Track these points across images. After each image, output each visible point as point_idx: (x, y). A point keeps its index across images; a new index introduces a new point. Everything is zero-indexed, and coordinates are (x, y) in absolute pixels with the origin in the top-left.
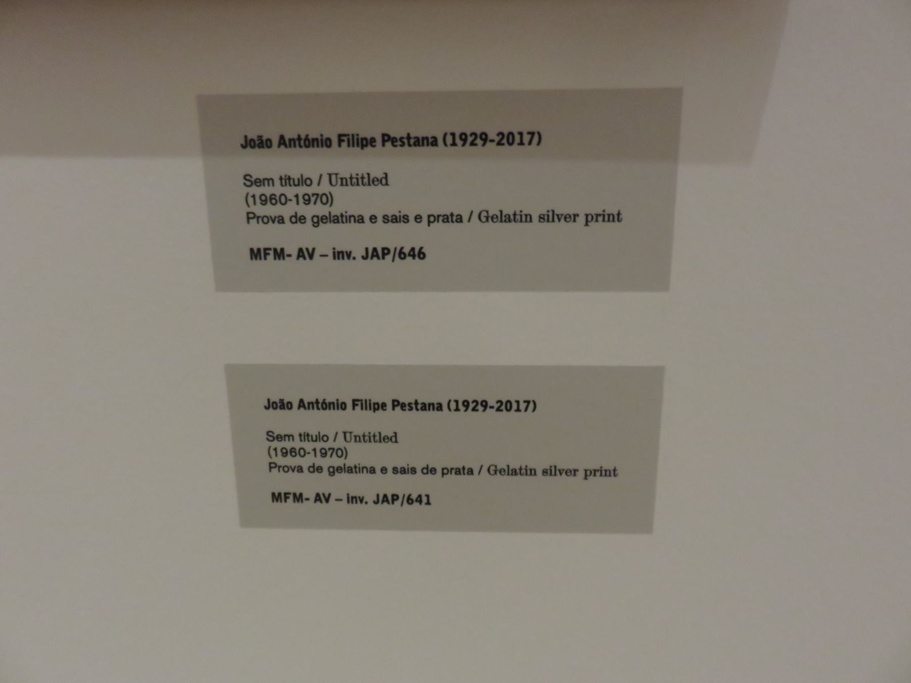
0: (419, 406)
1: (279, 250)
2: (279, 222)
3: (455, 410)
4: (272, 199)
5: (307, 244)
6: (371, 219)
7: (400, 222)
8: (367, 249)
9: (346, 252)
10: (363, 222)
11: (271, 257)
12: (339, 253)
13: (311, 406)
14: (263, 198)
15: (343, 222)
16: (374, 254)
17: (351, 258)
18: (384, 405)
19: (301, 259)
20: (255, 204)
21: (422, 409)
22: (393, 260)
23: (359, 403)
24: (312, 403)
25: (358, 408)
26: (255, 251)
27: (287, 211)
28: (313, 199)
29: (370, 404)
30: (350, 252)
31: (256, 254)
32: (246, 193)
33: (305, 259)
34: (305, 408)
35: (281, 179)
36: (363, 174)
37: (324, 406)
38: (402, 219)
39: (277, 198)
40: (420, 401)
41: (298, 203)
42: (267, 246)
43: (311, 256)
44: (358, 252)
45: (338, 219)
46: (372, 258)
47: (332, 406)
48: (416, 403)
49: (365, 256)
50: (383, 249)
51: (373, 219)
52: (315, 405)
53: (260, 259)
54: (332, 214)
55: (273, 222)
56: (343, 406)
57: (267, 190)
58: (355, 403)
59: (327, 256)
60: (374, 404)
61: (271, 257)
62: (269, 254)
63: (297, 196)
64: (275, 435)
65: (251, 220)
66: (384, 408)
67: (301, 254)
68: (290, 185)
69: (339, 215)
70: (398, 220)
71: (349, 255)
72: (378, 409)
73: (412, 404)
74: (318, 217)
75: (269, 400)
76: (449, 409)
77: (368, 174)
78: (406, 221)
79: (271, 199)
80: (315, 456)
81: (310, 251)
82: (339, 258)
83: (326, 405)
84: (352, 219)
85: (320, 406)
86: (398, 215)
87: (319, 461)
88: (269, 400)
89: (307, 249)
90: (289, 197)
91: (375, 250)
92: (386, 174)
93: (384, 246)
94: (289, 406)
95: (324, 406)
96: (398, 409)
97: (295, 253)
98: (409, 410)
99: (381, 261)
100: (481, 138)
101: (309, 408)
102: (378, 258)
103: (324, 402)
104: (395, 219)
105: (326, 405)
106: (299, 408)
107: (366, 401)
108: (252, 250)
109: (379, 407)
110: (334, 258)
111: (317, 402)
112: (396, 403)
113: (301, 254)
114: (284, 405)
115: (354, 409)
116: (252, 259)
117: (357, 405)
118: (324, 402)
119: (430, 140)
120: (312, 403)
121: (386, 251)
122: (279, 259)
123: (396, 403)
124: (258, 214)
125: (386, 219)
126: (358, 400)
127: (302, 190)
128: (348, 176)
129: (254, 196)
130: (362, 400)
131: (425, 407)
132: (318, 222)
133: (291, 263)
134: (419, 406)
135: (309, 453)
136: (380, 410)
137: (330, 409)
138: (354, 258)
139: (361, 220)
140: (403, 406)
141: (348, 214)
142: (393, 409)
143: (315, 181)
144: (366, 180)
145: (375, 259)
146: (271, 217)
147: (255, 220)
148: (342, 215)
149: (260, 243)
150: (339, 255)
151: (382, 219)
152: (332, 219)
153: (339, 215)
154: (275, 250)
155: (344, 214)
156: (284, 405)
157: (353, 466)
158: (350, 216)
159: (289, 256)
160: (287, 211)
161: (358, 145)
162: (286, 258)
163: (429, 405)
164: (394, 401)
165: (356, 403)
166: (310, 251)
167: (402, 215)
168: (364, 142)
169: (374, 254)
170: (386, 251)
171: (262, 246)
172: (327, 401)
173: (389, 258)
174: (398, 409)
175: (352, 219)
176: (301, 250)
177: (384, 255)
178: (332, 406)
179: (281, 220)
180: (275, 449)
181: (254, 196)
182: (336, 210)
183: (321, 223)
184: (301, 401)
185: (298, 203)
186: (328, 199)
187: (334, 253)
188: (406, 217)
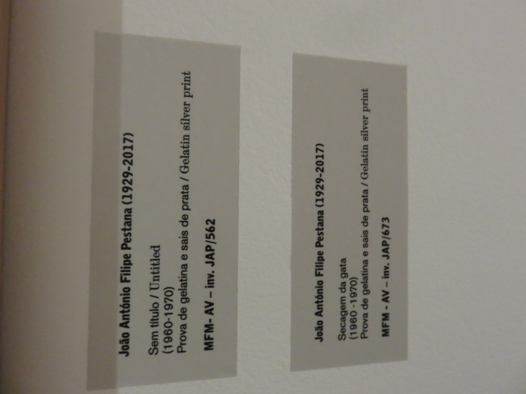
1: (206, 329)
2: (185, 328)
3: (323, 202)
4: (168, 333)
6: (184, 259)
7: (187, 237)
8: (207, 262)
9: (209, 278)
10: (186, 265)
11: (211, 335)
12: (209, 283)
13: (320, 307)
14: (167, 340)
15: (186, 280)
16: (210, 257)
18: (320, 254)
19: (213, 312)
20: (171, 346)
21: (322, 225)
22: (215, 243)
23: (318, 271)
25: (322, 272)
26: (206, 346)
27: (177, 322)
28: (169, 302)
29: (319, 263)
30: (209, 275)
31: (209, 346)
33: (212, 309)
34: (322, 311)
35: (152, 326)
36: (151, 264)
37: (320, 297)
38: (185, 236)
39: (167, 329)
41: (171, 314)
43: (211, 304)
44: (209, 269)
46: (213, 259)
47: (320, 291)
48: (318, 229)
49: (212, 264)
50: (207, 250)
53: (212, 343)
54: (181, 288)
55: (185, 332)
56: (320, 283)
57: (161, 337)
58: (318, 275)
59: (211, 293)
60: (319, 260)
61: (211, 335)
62: (209, 336)
63: (166, 314)
64: (341, 334)
65: (184, 350)
66: (321, 253)
67: (209, 312)
68: (158, 319)
69: (180, 283)
70: (185, 239)
71: (211, 276)
72: (322, 257)
73: (318, 233)
74: (182, 299)
75: (316, 338)
76: (322, 206)
77: (151, 260)
79: (168, 334)
81: (207, 305)
82: (213, 283)
83: (320, 296)
84: (184, 273)
85: (320, 300)
86: (181, 239)
88: (316, 338)
89: (206, 307)
90: (167, 321)
91: (207, 256)
92: (152, 247)
94: (320, 323)
95: (320, 297)
96: (322, 243)
97: (209, 316)
98: (323, 235)
100: (127, 176)
102: (213, 254)
103: (317, 297)
104: (185, 241)
105: (320, 296)
106: (322, 316)
107: (316, 266)
108: (206, 349)
109: (321, 257)
110: (213, 287)
112: (318, 244)
113: (209, 312)
114: (320, 327)
116: (212, 349)
117: (319, 273)
118: (317, 297)
119: (127, 214)
120: (318, 306)
121: (208, 248)
124: (179, 345)
125: (185, 248)
126: (316, 272)
127: (162, 310)
128: (152, 276)
129: (166, 347)
130: (316, 269)
131: (321, 223)
132: (186, 298)
133: (216, 319)
134: (320, 227)
136: (323, 256)
137: (322, 293)
138: (213, 272)
140: (320, 239)
141: (180, 276)
142: (322, 246)
143: (155, 300)
144: (156, 262)
145: (214, 256)
146: (181, 334)
147: (183, 346)
148: (181, 280)
150: (210, 283)
152: (184, 288)
153: (180, 283)
154: (206, 331)
155: (180, 279)
156: (320, 327)
158: (182, 274)
159: (210, 321)
160: (177, 322)
161: (129, 268)
163: (319, 220)
164: (317, 246)
165: (318, 273)
166: (207, 305)
167: (181, 236)
168: (127, 263)
169: (210, 257)
170: (208, 248)
171: (203, 341)
172: (317, 295)
173: (213, 246)
174: (322, 243)
175: (184, 273)
176: (206, 312)
177: (211, 250)
178: (320, 291)
179: (184, 326)
180: (351, 334)
182: (177, 285)
183: (187, 297)
184: (317, 314)
185: (171, 314)
186: (169, 290)
187: (209, 287)
188: (183, 233)
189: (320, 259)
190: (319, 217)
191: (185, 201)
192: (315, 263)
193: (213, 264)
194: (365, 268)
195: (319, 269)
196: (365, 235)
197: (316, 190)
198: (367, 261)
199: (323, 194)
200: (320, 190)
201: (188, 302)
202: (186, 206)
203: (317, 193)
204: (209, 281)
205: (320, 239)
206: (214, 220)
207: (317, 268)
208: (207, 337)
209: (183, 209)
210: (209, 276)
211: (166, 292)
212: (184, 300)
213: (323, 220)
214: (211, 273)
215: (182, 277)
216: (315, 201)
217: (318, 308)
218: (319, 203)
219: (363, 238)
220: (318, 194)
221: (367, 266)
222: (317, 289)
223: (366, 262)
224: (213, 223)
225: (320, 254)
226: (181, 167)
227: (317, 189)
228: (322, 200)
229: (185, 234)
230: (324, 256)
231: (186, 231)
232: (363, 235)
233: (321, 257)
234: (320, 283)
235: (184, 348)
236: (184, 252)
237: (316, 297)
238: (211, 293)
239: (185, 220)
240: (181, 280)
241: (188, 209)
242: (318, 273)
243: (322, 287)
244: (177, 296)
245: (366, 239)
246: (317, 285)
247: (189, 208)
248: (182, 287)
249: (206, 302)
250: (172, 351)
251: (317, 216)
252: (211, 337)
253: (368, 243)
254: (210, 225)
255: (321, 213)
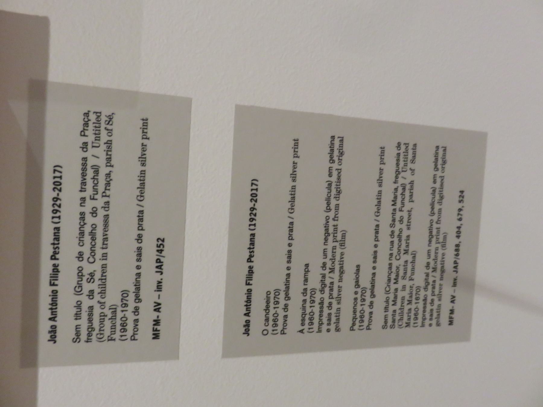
0: (252, 247)
1: (154, 323)
2: (138, 322)
5: (152, 307)
6: (138, 269)
9: (158, 284)
12: (158, 288)
16: (160, 268)
17: (161, 281)
18: (251, 268)
19: (160, 310)
23: (248, 281)
24: (247, 308)
25: (251, 282)
26: (154, 336)
28: (125, 302)
30: (158, 281)
31: (156, 336)
32: (120, 341)
33: (160, 308)
40: (249, 246)
42: (152, 329)
43: (159, 304)
44: (158, 277)
45: (138, 288)
46: (162, 269)
47: (249, 297)
48: (250, 248)
49: (160, 273)
50: (157, 262)
51: (138, 267)
52: (248, 307)
54: (135, 291)
55: (137, 325)
59: (159, 295)
60: (249, 273)
61: (159, 328)
62: (156, 329)
63: (122, 311)
65: (136, 338)
66: (252, 267)
67: (157, 310)
69: (135, 287)
71: (160, 282)
78: (140, 249)
79: (123, 326)
80: (278, 308)
83: (249, 301)
85: (249, 304)
86: (136, 253)
87: (281, 305)
89: (155, 306)
90: (123, 316)
91: (157, 267)
93: (155, 261)
95: (249, 302)
96: (252, 259)
97: (157, 314)
98: (254, 253)
99: (164, 264)
101: (250, 310)
102: (162, 265)
104: (139, 255)
105: (249, 301)
107: (247, 278)
108: (154, 338)
110: (161, 291)
111: (246, 305)
112: (249, 260)
113: (157, 310)
115: (251, 285)
117: (249, 283)
121: (158, 261)
122: (159, 323)
123: (249, 260)
124: (132, 334)
126: (246, 282)
131: (252, 243)
133: (163, 316)
134: (252, 247)
135: (276, 311)
138: (162, 279)
139: (139, 275)
140: (251, 256)
142: (253, 262)
145: (162, 267)
149: (150, 334)
150: (159, 287)
151: (139, 262)
152: (137, 291)
153: (135, 287)
154: (154, 325)
155: (134, 284)
157: (285, 286)
158: (136, 281)
159: (158, 317)
162: (159, 318)
163: (251, 241)
164: (248, 261)
165: (248, 283)
166: (156, 304)
169: (160, 268)
170: (158, 261)
171: (152, 333)
173: (162, 259)
176: (155, 310)
177: (160, 262)
178: (249, 297)
179: (136, 321)
181: (121, 336)
182: (132, 289)
185: (126, 311)
187: (158, 291)
189: (251, 272)
190: (251, 239)
191: (140, 223)
192: (245, 275)
193: (162, 273)
194: (288, 279)
195: (249, 280)
196: (289, 253)
197: (250, 217)
198: (289, 274)
199: (255, 220)
200: (253, 216)
201: (141, 302)
202: (140, 227)
203: (250, 219)
204: (158, 286)
205: (251, 256)
206: (164, 239)
207: (248, 279)
208: (155, 329)
209: (139, 230)
210: (158, 282)
211: (123, 294)
212: (137, 301)
213: (254, 241)
214: (160, 280)
215: (136, 283)
216: (248, 226)
217: (247, 310)
218: (252, 227)
219: (287, 256)
220: (252, 220)
221: (289, 278)
222: (247, 295)
223: (288, 275)
224: (163, 241)
225: (251, 268)
226: (138, 196)
227: (251, 216)
228: (255, 225)
229: (139, 249)
230: (254, 269)
231: (140, 247)
232: (287, 253)
233: (251, 271)
234: (249, 291)
235: (136, 337)
236: (138, 263)
237: (245, 301)
238: (159, 295)
239: (139, 238)
240: (135, 285)
241: (142, 230)
242: (248, 283)
243: (251, 294)
244: (131, 297)
245: (289, 257)
246: (247, 292)
247: (144, 229)
248: (136, 290)
249: (155, 303)
250: (127, 339)
251: (249, 238)
252: (158, 329)
253: (292, 260)
254: (160, 242)
255: (253, 235)
